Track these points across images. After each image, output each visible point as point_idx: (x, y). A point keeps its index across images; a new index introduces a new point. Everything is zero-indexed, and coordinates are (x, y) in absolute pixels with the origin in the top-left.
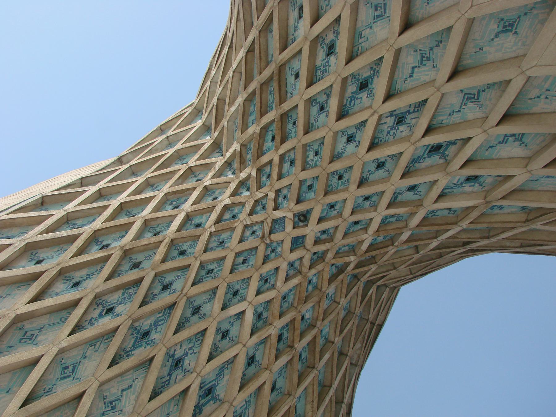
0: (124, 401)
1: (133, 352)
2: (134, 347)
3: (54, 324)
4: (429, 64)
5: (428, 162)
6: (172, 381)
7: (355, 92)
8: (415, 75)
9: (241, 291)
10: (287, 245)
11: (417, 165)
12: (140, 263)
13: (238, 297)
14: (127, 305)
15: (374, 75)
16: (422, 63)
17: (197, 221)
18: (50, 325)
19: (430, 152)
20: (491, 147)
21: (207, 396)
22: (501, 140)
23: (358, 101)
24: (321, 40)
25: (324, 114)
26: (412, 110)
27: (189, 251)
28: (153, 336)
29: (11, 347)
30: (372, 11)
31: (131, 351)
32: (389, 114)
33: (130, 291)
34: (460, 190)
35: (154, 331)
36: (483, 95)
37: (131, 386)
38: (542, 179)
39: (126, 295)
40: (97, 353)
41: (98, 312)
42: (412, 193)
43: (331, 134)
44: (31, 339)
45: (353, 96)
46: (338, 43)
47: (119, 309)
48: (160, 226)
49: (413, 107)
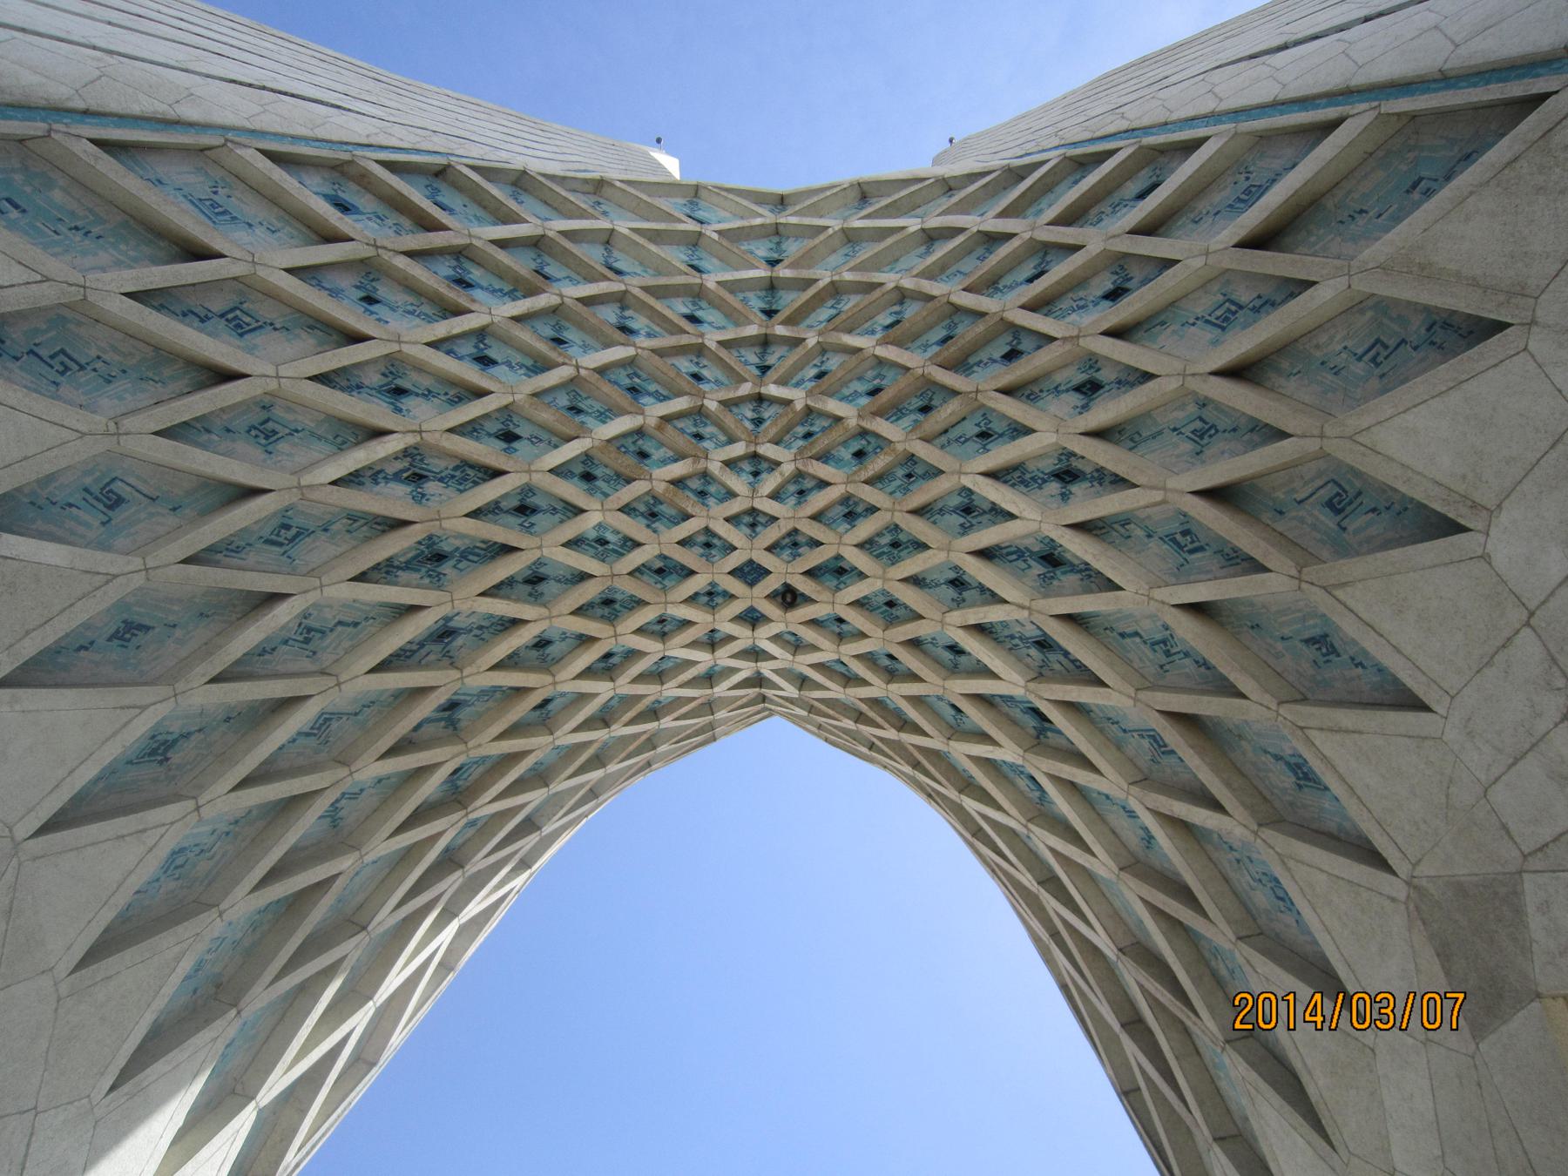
0: (328, 641)
1: (400, 573)
2: (407, 566)
3: (320, 438)
4: (1164, 660)
6: (417, 657)
8: (1128, 640)
9: (617, 606)
10: (737, 608)
12: (517, 437)
13: (606, 611)
14: (447, 491)
15: (1080, 571)
16: (1153, 644)
17: (647, 446)
18: (312, 434)
21: (445, 710)
25: (962, 520)
27: (599, 483)
28: (447, 568)
29: (228, 430)
30: (1175, 527)
31: (399, 568)
33: (470, 472)
35: (452, 562)
37: (356, 624)
39: (457, 473)
40: (348, 536)
41: (399, 465)
44: (267, 437)
47: (431, 487)
48: (589, 402)
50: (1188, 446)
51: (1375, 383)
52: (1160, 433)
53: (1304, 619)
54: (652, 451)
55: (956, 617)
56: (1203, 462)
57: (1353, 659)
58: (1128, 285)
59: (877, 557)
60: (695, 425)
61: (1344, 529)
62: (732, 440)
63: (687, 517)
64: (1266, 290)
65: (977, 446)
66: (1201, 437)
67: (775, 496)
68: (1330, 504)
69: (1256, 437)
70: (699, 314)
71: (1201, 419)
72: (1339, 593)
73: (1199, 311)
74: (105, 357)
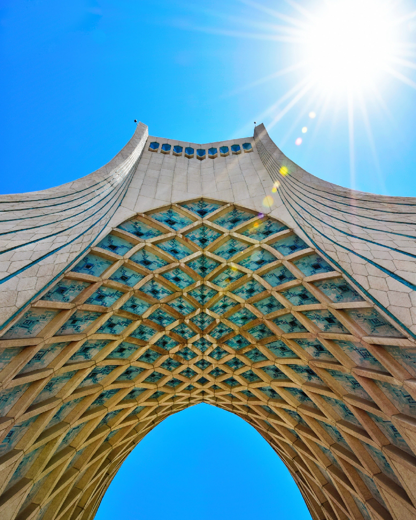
9: (158, 394)
25: (274, 373)
27: (151, 357)
28: (105, 398)
37: (78, 427)
47: (99, 376)
48: (146, 328)
50: (351, 384)
54: (168, 341)
58: (334, 320)
59: (245, 378)
60: (182, 328)
62: (194, 334)
63: (181, 364)
65: (281, 352)
66: (355, 384)
67: (211, 355)
70: (179, 276)
74: (5, 394)
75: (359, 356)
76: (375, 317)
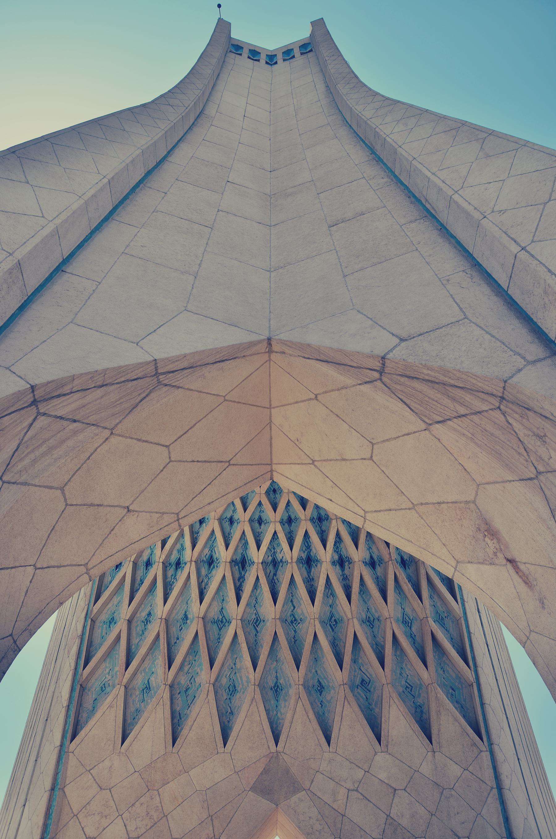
4: (289, 620)
5: (240, 551)
7: (310, 552)
8: (291, 604)
11: (243, 542)
15: (309, 577)
19: (244, 557)
20: (223, 600)
22: (223, 611)
23: (304, 548)
24: (351, 561)
25: (315, 518)
26: (275, 578)
30: (337, 617)
32: (284, 560)
34: (208, 546)
36: (254, 632)
38: (186, 607)
42: (228, 517)
43: (303, 517)
45: (309, 548)
46: (340, 571)
49: (276, 581)
50: (364, 617)
51: (401, 689)
52: (366, 603)
53: (325, 678)
55: (279, 528)
56: (361, 625)
57: (322, 701)
58: (407, 567)
61: (357, 688)
64: (418, 639)
66: (368, 621)
68: (363, 680)
69: (375, 646)
71: (374, 619)
72: (346, 703)
73: (406, 609)
75: (400, 615)
76: (444, 617)
